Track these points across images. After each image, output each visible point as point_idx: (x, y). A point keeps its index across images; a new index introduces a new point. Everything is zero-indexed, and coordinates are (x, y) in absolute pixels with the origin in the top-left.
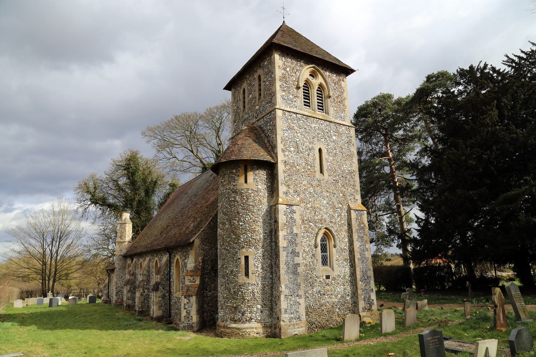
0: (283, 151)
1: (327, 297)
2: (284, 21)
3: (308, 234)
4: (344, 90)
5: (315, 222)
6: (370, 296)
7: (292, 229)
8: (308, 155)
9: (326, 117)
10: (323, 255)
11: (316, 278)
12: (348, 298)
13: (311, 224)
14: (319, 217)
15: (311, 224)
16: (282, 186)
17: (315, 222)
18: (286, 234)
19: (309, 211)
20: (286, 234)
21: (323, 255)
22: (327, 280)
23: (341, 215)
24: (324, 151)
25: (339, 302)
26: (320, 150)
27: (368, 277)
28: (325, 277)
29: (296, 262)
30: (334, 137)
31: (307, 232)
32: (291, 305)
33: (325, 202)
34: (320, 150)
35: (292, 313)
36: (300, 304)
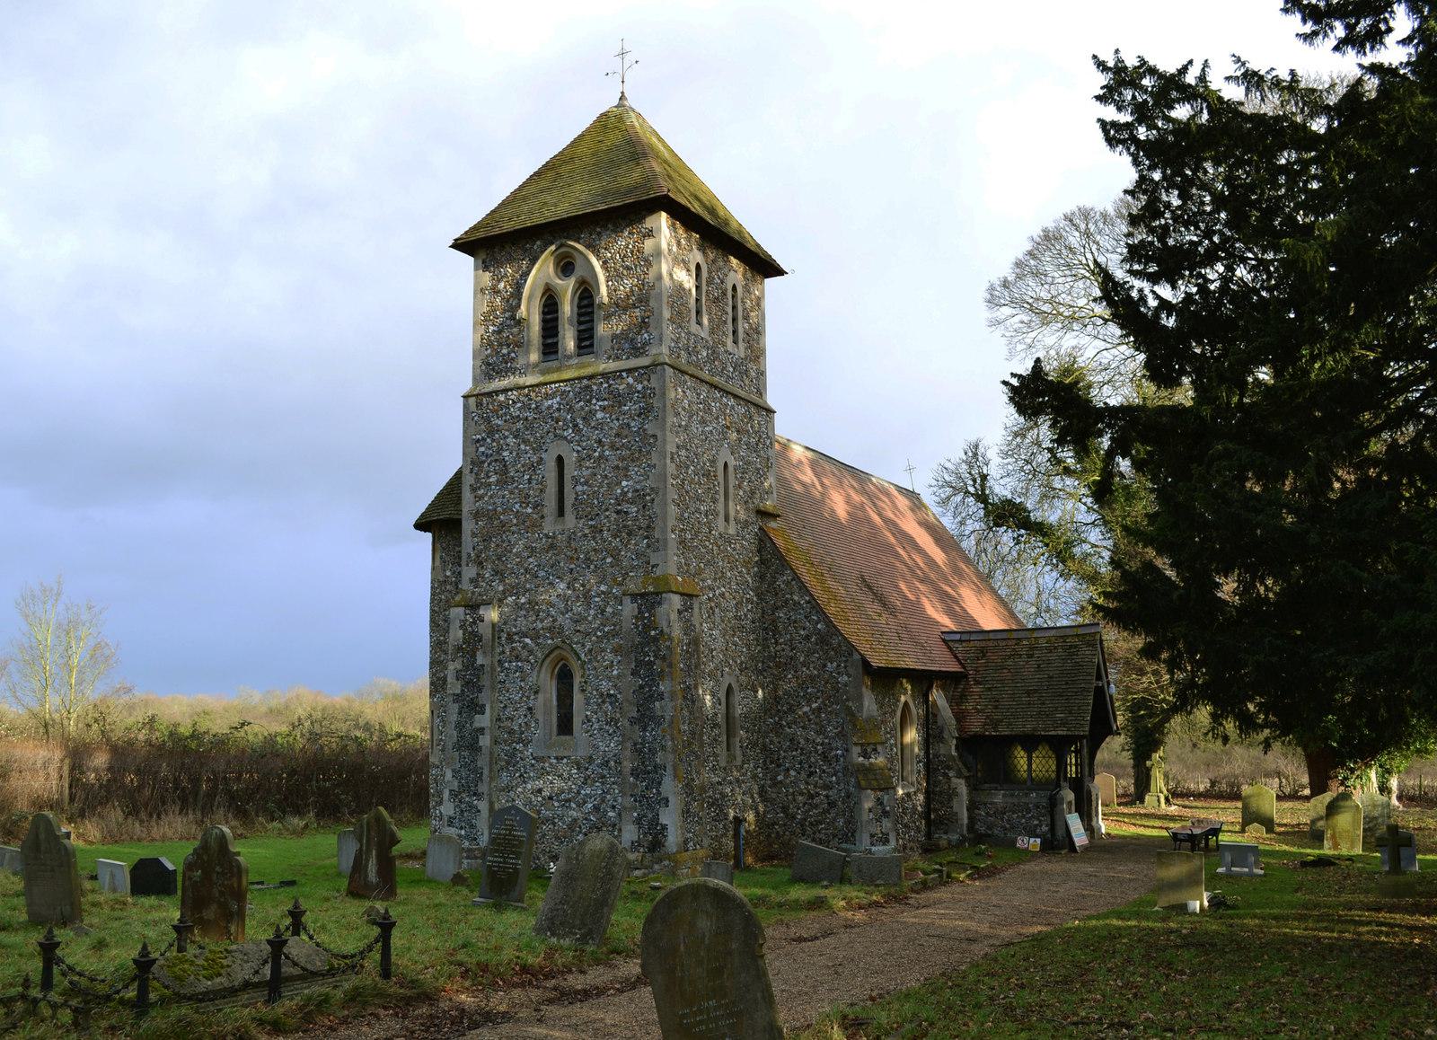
0: (474, 490)
1: (556, 804)
2: (622, 93)
3: (520, 664)
6: (658, 815)
7: (474, 656)
8: (530, 480)
11: (533, 762)
12: (611, 814)
13: (528, 640)
14: (547, 623)
15: (528, 640)
16: (467, 565)
17: (536, 637)
18: (459, 667)
19: (523, 612)
20: (459, 667)
23: (603, 611)
24: (571, 459)
25: (586, 819)
26: (560, 460)
27: (655, 767)
29: (477, 725)
30: (600, 415)
31: (518, 658)
32: (462, 811)
34: (560, 460)
35: (461, 828)
36: (479, 811)
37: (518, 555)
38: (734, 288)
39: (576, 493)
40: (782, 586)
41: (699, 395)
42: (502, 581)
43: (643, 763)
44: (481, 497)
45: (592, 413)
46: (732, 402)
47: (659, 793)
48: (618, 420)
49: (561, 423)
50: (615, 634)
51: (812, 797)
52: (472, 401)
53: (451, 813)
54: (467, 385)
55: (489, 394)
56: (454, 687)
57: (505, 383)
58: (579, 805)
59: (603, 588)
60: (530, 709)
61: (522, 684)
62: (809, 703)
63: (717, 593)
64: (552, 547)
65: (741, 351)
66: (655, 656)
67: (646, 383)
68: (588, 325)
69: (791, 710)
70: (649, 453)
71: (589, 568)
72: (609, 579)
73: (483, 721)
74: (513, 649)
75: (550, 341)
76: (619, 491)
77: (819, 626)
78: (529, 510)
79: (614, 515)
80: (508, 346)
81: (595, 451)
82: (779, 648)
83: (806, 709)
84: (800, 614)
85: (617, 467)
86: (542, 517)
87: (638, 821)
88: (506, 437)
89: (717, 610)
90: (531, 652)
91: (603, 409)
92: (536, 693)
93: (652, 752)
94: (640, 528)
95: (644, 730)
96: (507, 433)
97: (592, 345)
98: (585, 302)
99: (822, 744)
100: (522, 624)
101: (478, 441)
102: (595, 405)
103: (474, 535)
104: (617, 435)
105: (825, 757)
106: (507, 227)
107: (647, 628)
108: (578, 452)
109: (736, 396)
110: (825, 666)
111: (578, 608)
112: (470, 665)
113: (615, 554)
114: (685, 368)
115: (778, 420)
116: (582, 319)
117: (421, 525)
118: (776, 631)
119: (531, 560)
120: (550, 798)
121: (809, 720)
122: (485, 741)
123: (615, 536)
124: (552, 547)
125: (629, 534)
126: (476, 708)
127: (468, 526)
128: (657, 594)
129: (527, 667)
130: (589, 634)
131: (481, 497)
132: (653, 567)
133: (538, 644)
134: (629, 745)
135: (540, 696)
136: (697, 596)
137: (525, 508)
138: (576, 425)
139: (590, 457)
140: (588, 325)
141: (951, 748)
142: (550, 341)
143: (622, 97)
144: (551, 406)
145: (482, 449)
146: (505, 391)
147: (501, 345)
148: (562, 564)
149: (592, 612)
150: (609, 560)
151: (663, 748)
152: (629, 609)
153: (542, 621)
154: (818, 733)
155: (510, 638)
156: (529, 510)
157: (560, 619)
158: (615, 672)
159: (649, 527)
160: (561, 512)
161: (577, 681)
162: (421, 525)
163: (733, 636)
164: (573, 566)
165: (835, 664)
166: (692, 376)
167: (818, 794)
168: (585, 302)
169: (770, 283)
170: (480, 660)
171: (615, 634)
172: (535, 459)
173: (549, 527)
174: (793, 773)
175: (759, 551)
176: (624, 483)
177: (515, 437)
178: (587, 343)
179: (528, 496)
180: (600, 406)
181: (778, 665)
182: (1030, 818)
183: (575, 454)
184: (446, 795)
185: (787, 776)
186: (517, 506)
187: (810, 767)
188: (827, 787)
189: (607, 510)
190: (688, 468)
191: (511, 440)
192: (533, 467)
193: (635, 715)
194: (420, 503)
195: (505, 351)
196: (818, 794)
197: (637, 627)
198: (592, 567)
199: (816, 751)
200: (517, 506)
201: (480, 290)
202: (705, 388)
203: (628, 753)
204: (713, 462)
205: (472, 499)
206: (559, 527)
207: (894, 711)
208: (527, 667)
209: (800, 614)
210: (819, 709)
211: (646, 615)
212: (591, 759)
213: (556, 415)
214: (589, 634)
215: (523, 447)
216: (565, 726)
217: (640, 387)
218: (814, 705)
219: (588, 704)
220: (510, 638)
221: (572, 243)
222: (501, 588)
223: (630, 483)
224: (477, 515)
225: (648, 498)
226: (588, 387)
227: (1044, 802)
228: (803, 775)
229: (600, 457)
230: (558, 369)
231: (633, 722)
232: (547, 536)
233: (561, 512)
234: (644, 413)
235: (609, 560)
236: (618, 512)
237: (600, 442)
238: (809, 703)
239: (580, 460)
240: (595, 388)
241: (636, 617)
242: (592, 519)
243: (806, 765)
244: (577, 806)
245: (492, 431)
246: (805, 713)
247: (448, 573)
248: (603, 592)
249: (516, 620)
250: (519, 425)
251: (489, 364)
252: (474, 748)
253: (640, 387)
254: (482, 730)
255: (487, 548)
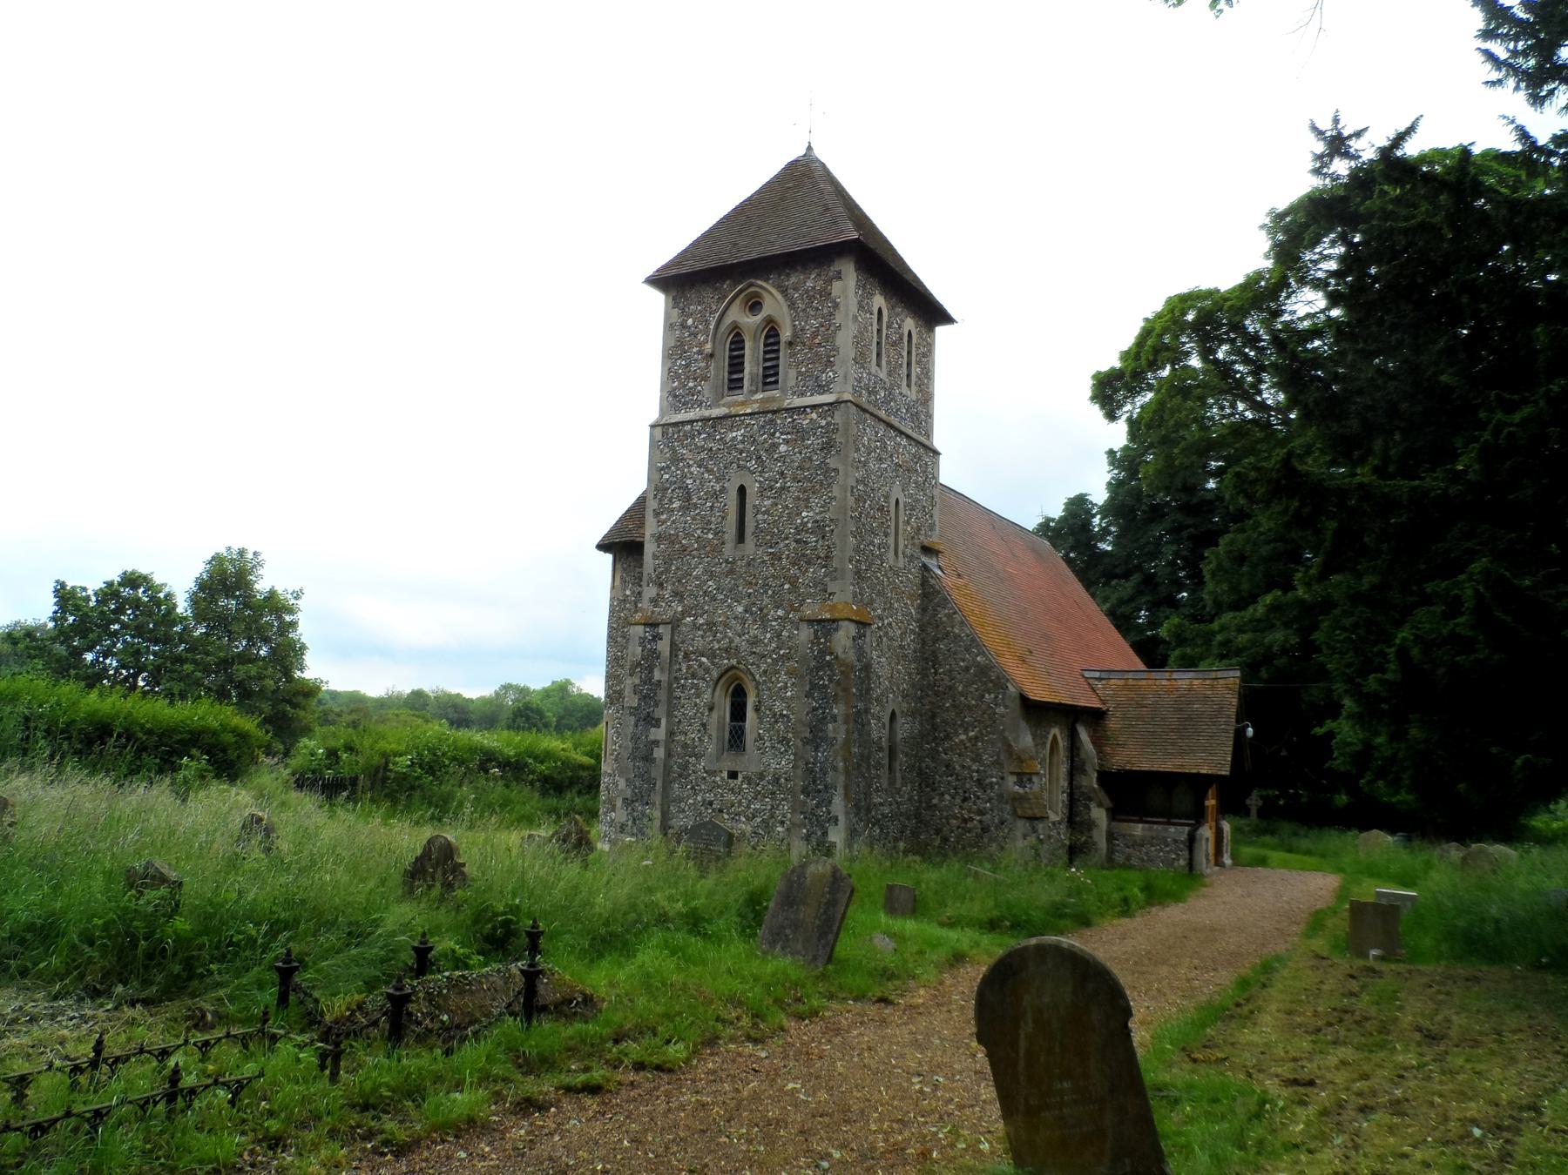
0: (657, 514)
1: (726, 816)
3: (696, 682)
4: (836, 306)
5: (712, 655)
7: (651, 671)
9: (773, 399)
10: (734, 727)
12: (780, 829)
13: (704, 660)
14: (724, 643)
15: (704, 660)
16: (648, 585)
17: (712, 655)
18: (637, 681)
19: (700, 633)
20: (637, 681)
21: (734, 727)
22: (730, 781)
23: (779, 636)
24: (753, 489)
25: (755, 833)
26: (742, 490)
28: (725, 775)
29: (652, 737)
30: (783, 448)
31: (694, 676)
32: (634, 819)
33: (740, 609)
34: (742, 490)
37: (697, 578)
38: (910, 333)
39: (757, 521)
40: (944, 619)
41: (877, 433)
42: (681, 601)
43: (814, 782)
44: (664, 522)
45: (775, 446)
46: (904, 442)
47: (829, 812)
48: (801, 453)
49: (744, 455)
50: (788, 657)
51: (965, 821)
52: (659, 431)
53: (623, 819)
54: (653, 414)
55: (676, 424)
56: (632, 700)
57: (691, 415)
58: (748, 819)
59: (780, 613)
60: (704, 725)
61: (698, 701)
62: (966, 731)
63: (886, 622)
64: (732, 572)
65: (913, 394)
66: (830, 680)
67: (829, 419)
68: (774, 363)
69: (948, 737)
70: (829, 485)
71: (766, 592)
72: (785, 604)
73: (659, 733)
74: (689, 667)
75: (735, 376)
76: (799, 521)
77: (979, 659)
78: (711, 536)
79: (794, 545)
80: (695, 379)
81: (777, 482)
82: (938, 677)
83: (963, 737)
84: (960, 646)
85: (798, 498)
86: (723, 543)
87: (807, 838)
88: (689, 466)
89: (885, 639)
90: (707, 671)
91: (787, 442)
92: (711, 709)
93: (824, 772)
94: (819, 558)
95: (816, 750)
96: (691, 462)
97: (776, 382)
98: (772, 340)
99: (977, 772)
100: (699, 643)
101: (662, 469)
102: (779, 438)
103: (655, 557)
104: (801, 468)
105: (979, 782)
106: (699, 266)
107: (823, 653)
108: (760, 482)
109: (908, 437)
110: (983, 696)
111: (754, 630)
112: (648, 680)
113: (793, 582)
114: (866, 406)
115: (943, 462)
116: (768, 356)
117: (603, 547)
118: (935, 662)
119: (710, 583)
120: (721, 811)
121: (966, 748)
122: (659, 753)
123: (793, 564)
124: (732, 572)
125: (809, 563)
126: (652, 721)
127: (650, 548)
128: (834, 621)
129: (702, 684)
130: (764, 656)
131: (664, 522)
132: (830, 594)
133: (713, 663)
134: (801, 764)
135: (715, 715)
136: (870, 625)
137: (706, 534)
138: (759, 457)
139: (771, 488)
140: (774, 363)
141: (1091, 780)
142: (735, 376)
143: (809, 148)
144: (735, 437)
145: (667, 476)
146: (691, 422)
147: (688, 378)
148: (740, 589)
149: (768, 635)
150: (786, 586)
151: (835, 769)
152: (805, 634)
153: (719, 642)
154: (974, 760)
155: (687, 656)
156: (711, 536)
157: (737, 640)
158: (789, 694)
159: (827, 557)
160: (741, 538)
161: (751, 701)
162: (603, 547)
163: (898, 664)
164: (751, 591)
165: (993, 696)
166: (872, 414)
167: (971, 819)
168: (772, 340)
169: (941, 331)
170: (657, 675)
171: (788, 657)
172: (718, 488)
173: (728, 550)
174: (947, 797)
175: (922, 585)
176: (804, 514)
177: (699, 466)
178: (773, 379)
179: (709, 522)
180: (784, 439)
181: (936, 694)
182: (1168, 852)
183: (757, 485)
184: (619, 803)
185: (941, 800)
186: (699, 532)
187: (965, 792)
188: (981, 812)
189: (787, 539)
190: (865, 502)
191: (694, 469)
192: (715, 495)
193: (807, 735)
194: (603, 525)
195: (691, 384)
196: (971, 819)
197: (813, 652)
198: (770, 592)
199: (972, 777)
200: (699, 532)
201: (669, 327)
202: (882, 427)
203: (799, 772)
204: (887, 497)
205: (655, 523)
206: (739, 554)
207: (1044, 743)
208: (702, 684)
209: (960, 646)
210: (976, 738)
211: (822, 640)
212: (761, 776)
213: (741, 446)
214: (764, 656)
215: (706, 475)
216: (736, 740)
217: (823, 423)
218: (971, 734)
219: (761, 722)
220: (687, 656)
221: (760, 282)
222: (680, 609)
223: (811, 514)
224: (659, 538)
225: (827, 529)
226: (772, 421)
227: (1184, 837)
228: (958, 800)
229: (782, 488)
230: (743, 404)
231: (806, 742)
232: (727, 561)
233: (741, 538)
234: (827, 447)
235: (786, 586)
236: (797, 541)
237: (782, 473)
238: (966, 731)
239: (762, 491)
240: (779, 422)
241: (813, 643)
242: (771, 547)
243: (960, 791)
244: (747, 820)
245: (676, 459)
246: (962, 741)
247: (628, 593)
248: (780, 617)
249: (693, 640)
250: (703, 455)
251: (676, 396)
252: (648, 758)
253: (823, 423)
254: (656, 743)
255: (667, 571)
